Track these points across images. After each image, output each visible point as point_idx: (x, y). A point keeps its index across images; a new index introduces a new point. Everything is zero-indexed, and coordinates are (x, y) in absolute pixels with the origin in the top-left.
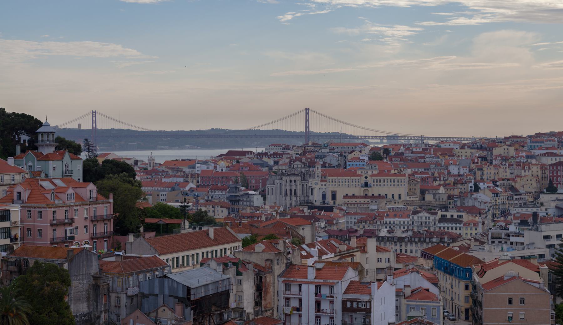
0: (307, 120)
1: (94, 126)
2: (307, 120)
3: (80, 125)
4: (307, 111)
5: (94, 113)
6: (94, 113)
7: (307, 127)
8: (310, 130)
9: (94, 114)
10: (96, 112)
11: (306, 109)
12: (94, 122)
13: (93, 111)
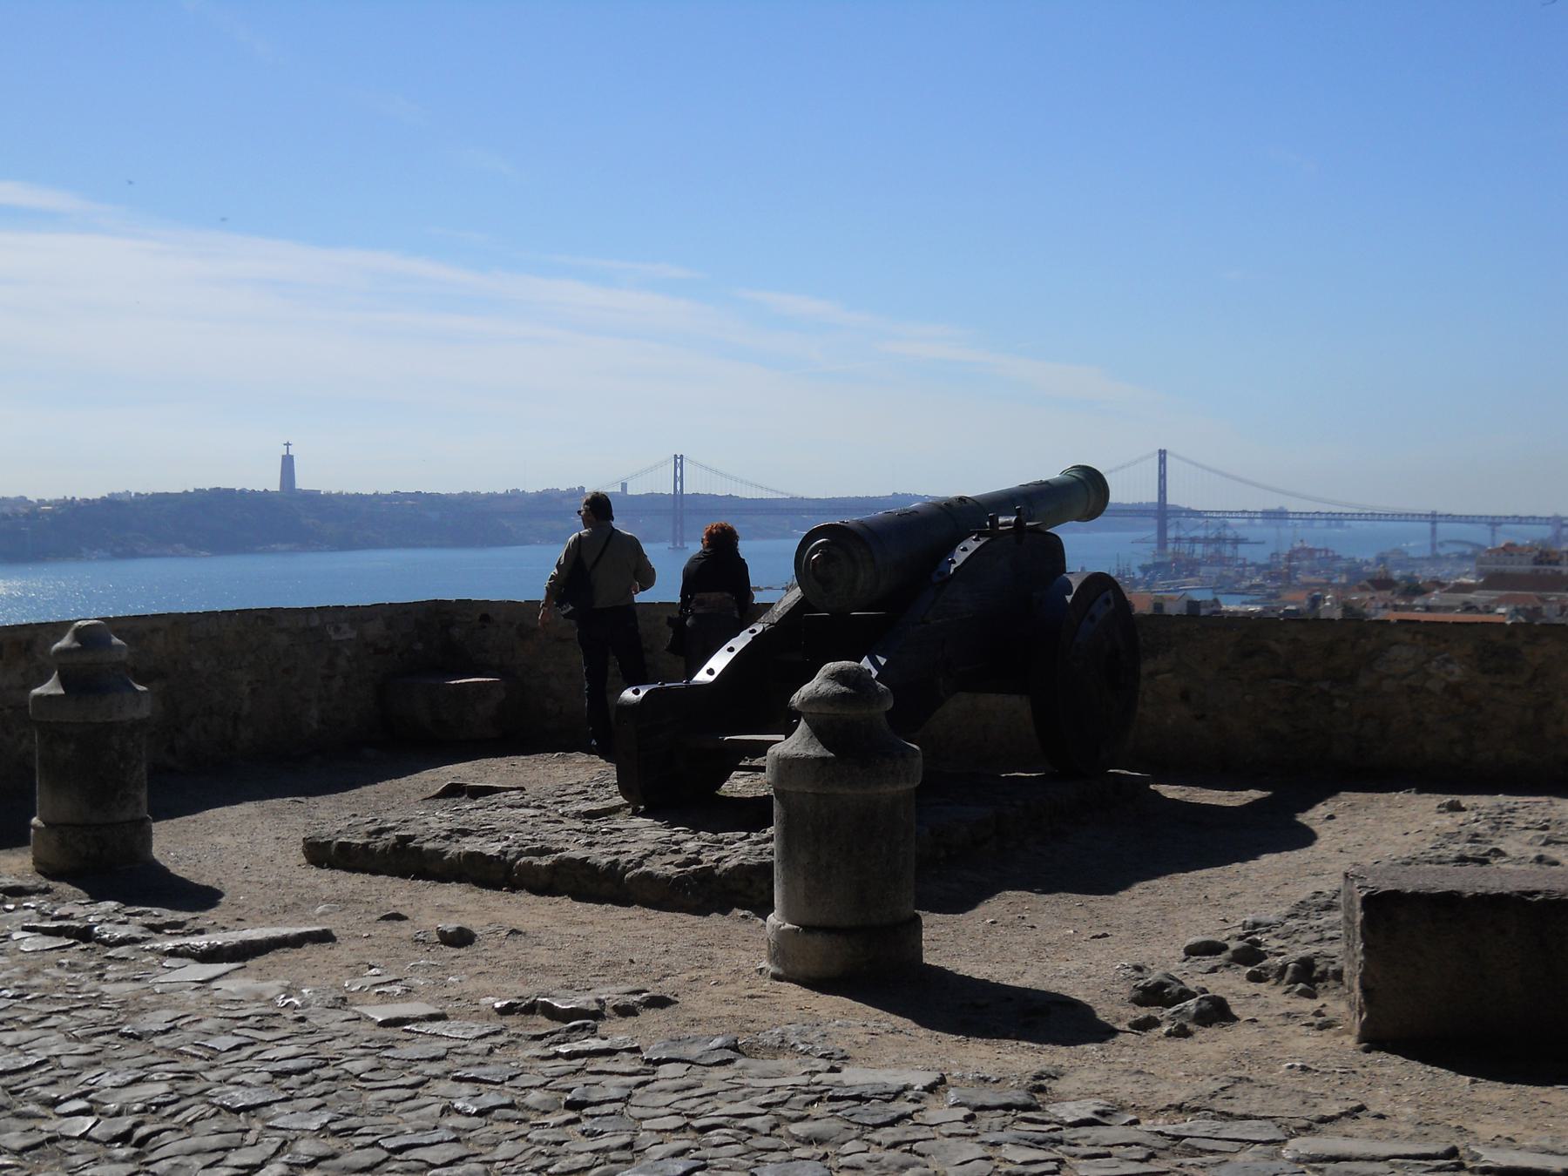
0: (1162, 477)
1: (678, 489)
2: (1162, 477)
3: (624, 486)
4: (1162, 454)
5: (679, 461)
6: (679, 461)
7: (1162, 491)
8: (1170, 501)
9: (679, 461)
10: (682, 456)
11: (1160, 450)
12: (678, 479)
13: (676, 456)
